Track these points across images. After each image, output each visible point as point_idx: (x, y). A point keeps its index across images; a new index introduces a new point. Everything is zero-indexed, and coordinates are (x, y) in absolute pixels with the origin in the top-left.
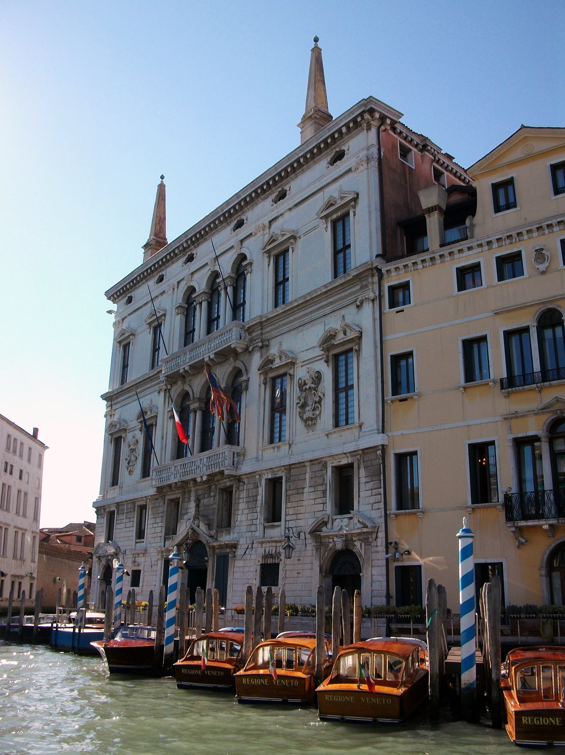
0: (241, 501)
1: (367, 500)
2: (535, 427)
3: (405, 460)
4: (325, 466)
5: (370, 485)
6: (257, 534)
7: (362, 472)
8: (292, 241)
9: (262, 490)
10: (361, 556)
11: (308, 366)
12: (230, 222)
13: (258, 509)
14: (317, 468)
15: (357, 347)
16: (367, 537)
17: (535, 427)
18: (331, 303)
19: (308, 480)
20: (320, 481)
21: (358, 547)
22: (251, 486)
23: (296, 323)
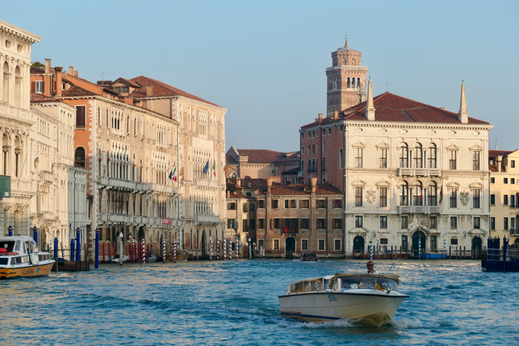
2: (514, 216)
3: (494, 218)
9: (449, 219)
16: (484, 235)
17: (514, 216)
21: (482, 236)
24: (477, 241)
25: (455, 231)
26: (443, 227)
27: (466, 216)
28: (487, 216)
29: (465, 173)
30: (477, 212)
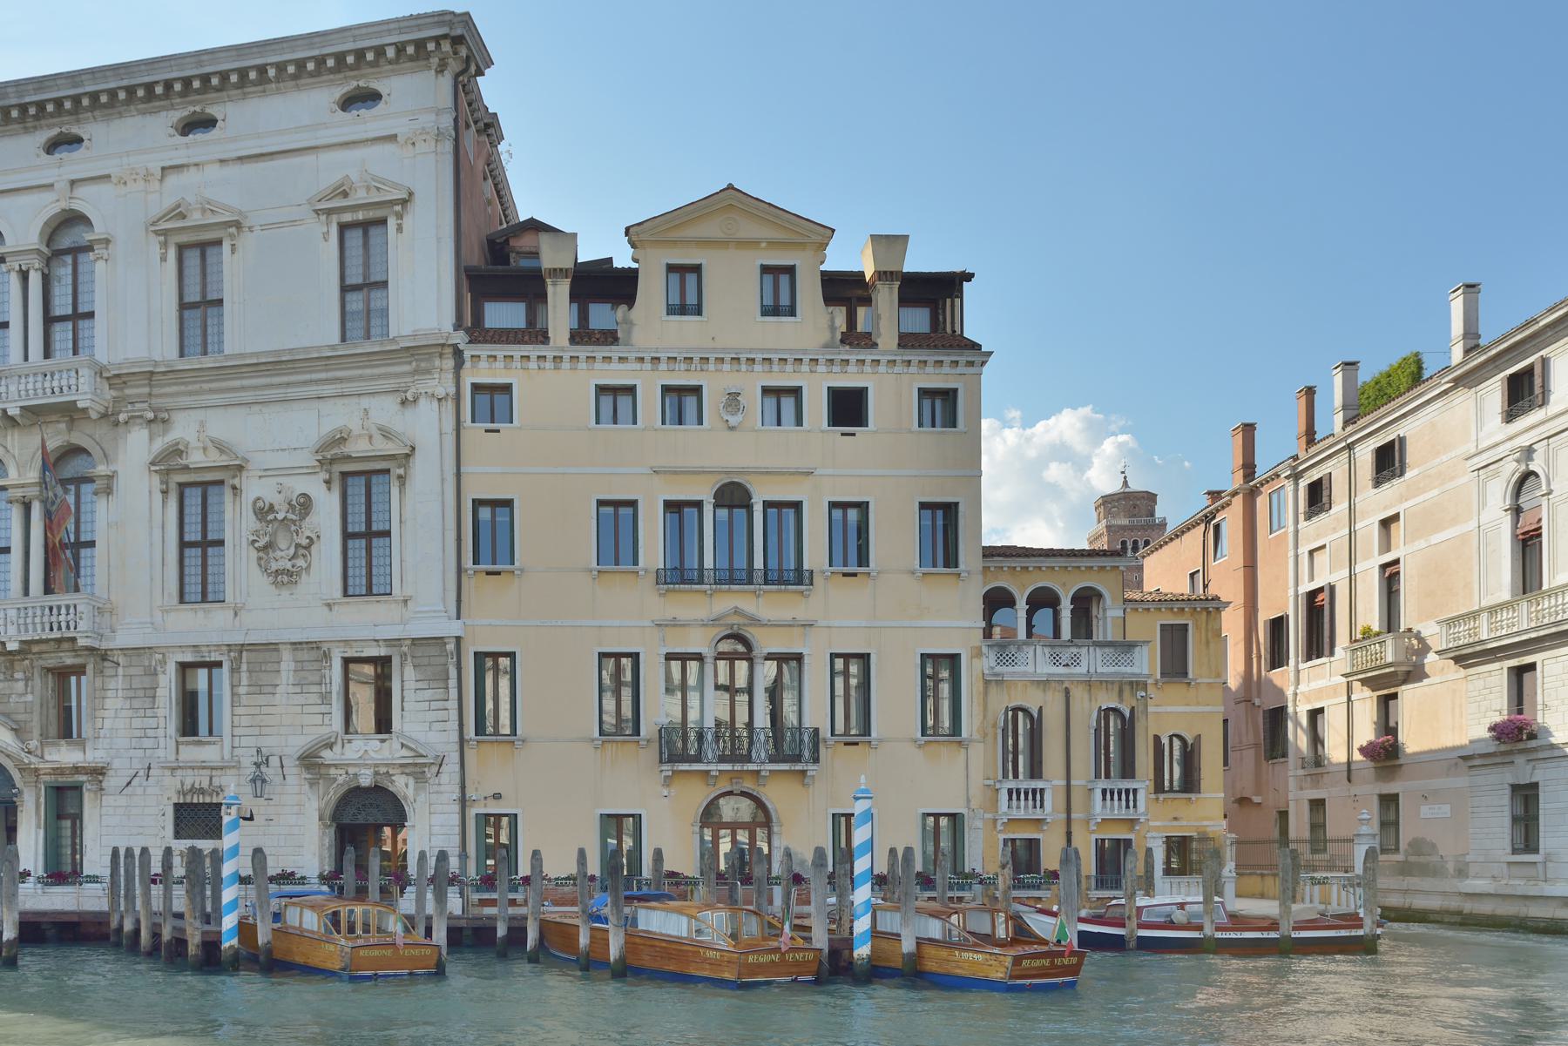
0: (109, 693)
1: (424, 718)
4: (327, 656)
5: (428, 694)
6: (161, 753)
7: (410, 672)
8: (233, 230)
10: (405, 798)
11: (280, 480)
12: (35, 128)
13: (161, 712)
14: (305, 655)
15: (401, 471)
18: (340, 380)
19: (284, 674)
20: (316, 679)
21: (402, 785)
22: (133, 671)
23: (248, 396)
24: (363, 820)
25: (209, 754)
26: (120, 726)
27: (286, 655)
28: (439, 641)
29: (280, 372)
30: (369, 625)
